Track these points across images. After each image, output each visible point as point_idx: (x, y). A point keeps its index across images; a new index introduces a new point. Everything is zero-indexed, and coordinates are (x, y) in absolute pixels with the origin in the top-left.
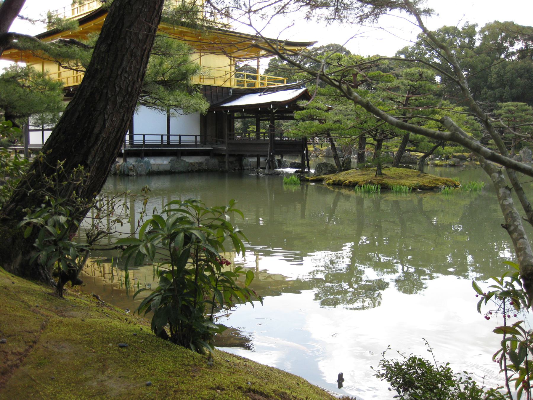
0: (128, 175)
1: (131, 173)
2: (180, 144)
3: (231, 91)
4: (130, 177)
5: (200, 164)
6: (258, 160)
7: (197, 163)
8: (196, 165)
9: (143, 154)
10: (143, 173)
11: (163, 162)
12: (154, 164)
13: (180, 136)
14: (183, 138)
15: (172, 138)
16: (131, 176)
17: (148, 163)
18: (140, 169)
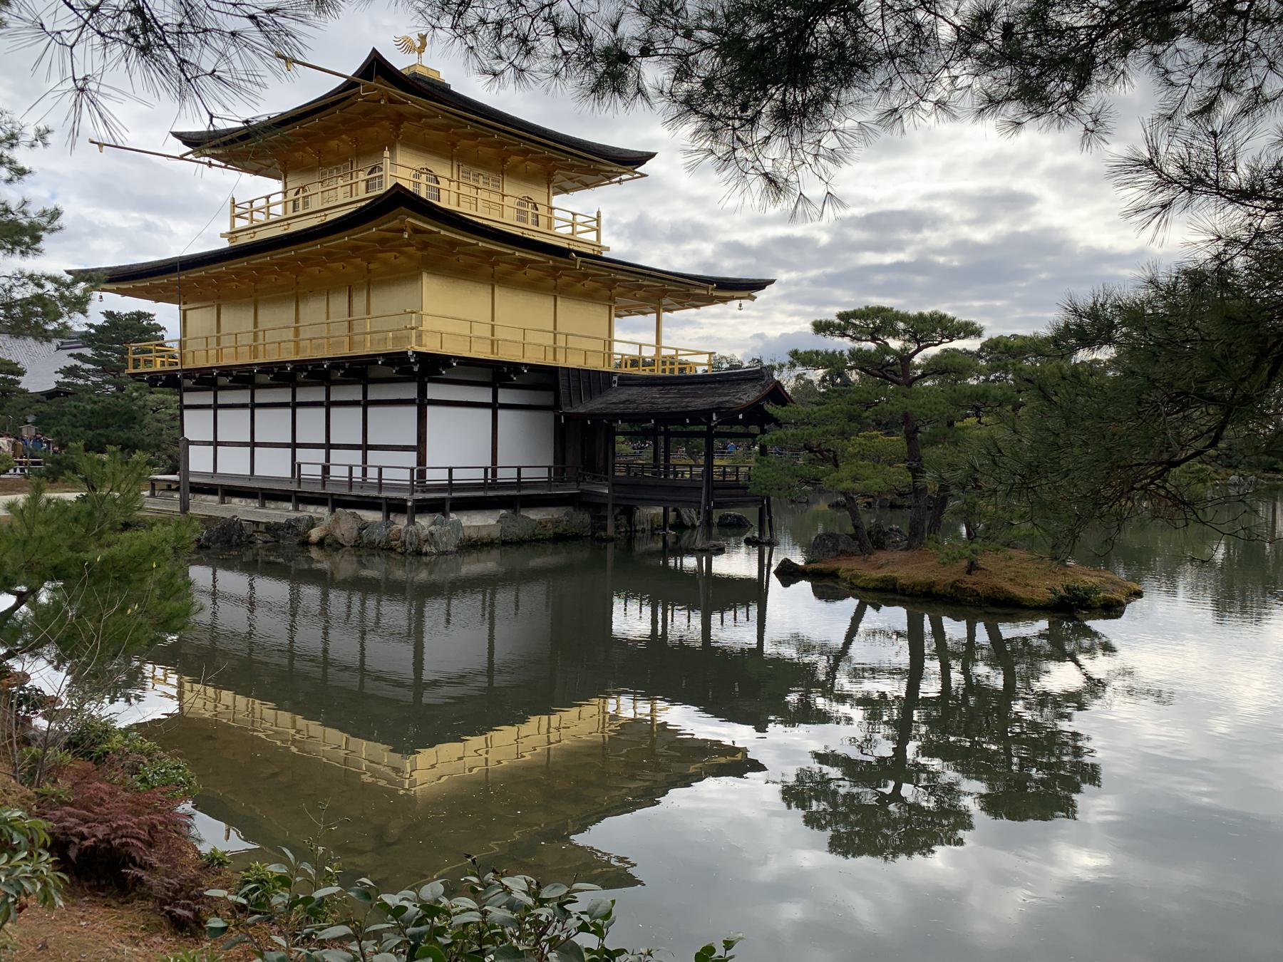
0: (419, 553)
1: (426, 548)
2: (519, 484)
3: (615, 378)
4: (425, 559)
5: (557, 522)
6: (665, 510)
7: (550, 521)
8: (549, 525)
9: (448, 508)
13: (519, 469)
14: (524, 473)
15: (501, 474)
16: (426, 554)
17: (458, 525)
18: (444, 539)
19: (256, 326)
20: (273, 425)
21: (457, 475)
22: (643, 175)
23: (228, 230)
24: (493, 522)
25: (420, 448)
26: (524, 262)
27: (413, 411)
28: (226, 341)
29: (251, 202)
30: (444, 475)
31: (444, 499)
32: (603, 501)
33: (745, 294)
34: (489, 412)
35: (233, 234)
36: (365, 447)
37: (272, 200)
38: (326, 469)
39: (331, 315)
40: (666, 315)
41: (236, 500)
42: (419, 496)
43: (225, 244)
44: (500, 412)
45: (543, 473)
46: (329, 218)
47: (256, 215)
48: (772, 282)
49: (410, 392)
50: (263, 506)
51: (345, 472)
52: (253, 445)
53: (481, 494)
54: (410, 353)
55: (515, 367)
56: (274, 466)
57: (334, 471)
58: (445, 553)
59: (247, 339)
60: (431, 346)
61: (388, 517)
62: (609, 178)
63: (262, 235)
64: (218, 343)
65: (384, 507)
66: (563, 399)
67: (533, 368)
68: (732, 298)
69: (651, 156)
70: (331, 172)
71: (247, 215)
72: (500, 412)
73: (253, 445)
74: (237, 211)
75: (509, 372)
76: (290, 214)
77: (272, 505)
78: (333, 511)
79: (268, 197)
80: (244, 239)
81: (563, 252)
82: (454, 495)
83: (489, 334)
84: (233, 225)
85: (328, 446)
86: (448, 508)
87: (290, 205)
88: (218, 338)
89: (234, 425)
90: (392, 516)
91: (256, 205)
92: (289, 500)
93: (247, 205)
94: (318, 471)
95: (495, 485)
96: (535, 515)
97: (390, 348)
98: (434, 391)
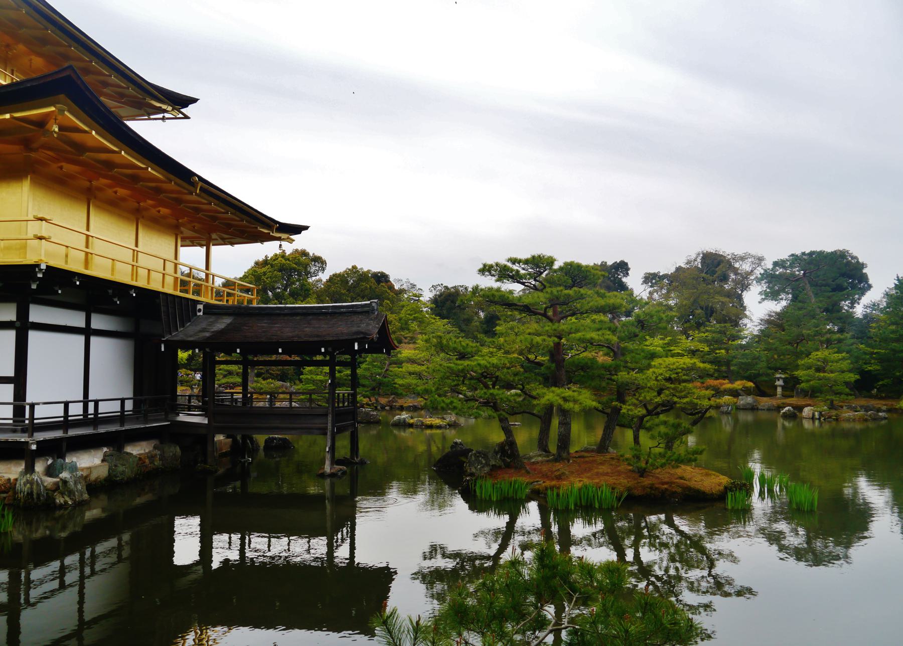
3: (200, 307)
5: (151, 457)
8: (147, 461)
10: (86, 496)
11: (89, 462)
17: (73, 468)
22: (186, 117)
30: (58, 411)
33: (284, 236)
34: (81, 339)
40: (214, 249)
42: (41, 436)
44: (94, 340)
48: (306, 228)
54: (43, 267)
55: (122, 289)
62: (149, 114)
68: (279, 239)
69: (194, 101)
72: (94, 340)
82: (72, 432)
86: (64, 449)
95: (98, 420)
98: (37, 314)
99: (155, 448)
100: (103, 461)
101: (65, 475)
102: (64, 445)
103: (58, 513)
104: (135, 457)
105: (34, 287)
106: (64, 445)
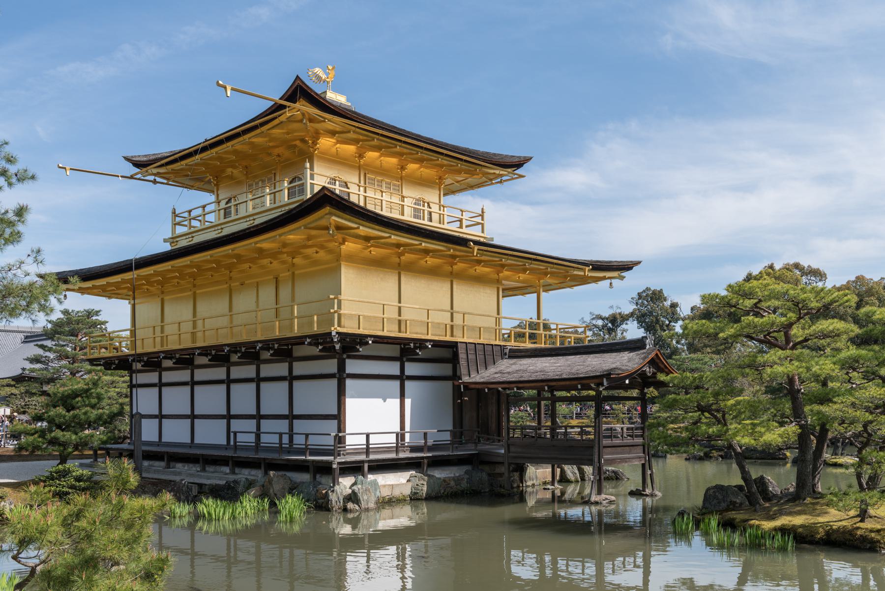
5: (457, 480)
7: (453, 479)
8: (452, 483)
10: (372, 505)
12: (384, 486)
16: (351, 511)
17: (375, 483)
19: (194, 315)
20: (210, 399)
21: (373, 439)
23: (170, 236)
24: (404, 481)
25: (339, 417)
26: (427, 252)
27: (334, 383)
28: (168, 330)
29: (190, 212)
31: (363, 462)
32: (500, 460)
35: (173, 240)
36: (291, 417)
37: (207, 209)
38: (258, 437)
39: (260, 304)
41: (179, 466)
43: (167, 247)
44: (408, 384)
45: (447, 436)
46: (257, 222)
47: (195, 223)
49: (331, 366)
50: (204, 470)
51: (275, 439)
52: (193, 417)
53: (393, 456)
54: (334, 333)
56: (211, 434)
57: (264, 438)
58: (367, 510)
59: (187, 327)
60: (349, 327)
61: (315, 478)
63: (198, 239)
64: (162, 331)
65: (311, 469)
66: (463, 370)
67: (437, 344)
70: (257, 183)
71: (186, 223)
72: (408, 384)
73: (193, 417)
74: (178, 219)
75: (415, 348)
76: (222, 220)
77: (210, 469)
78: (266, 473)
79: (204, 207)
80: (183, 243)
81: (462, 242)
82: (372, 457)
83: (396, 316)
84: (174, 230)
85: (259, 417)
87: (222, 212)
88: (162, 327)
89: (176, 400)
90: (318, 476)
91: (193, 214)
92: (227, 465)
93: (186, 215)
94: (252, 438)
96: (440, 474)
97: (315, 329)
98: (353, 366)
99: (466, 473)
100: (408, 481)
101: (355, 488)
102: (366, 466)
103: (350, 516)
104: (440, 479)
105: (338, 347)
106: (366, 466)
